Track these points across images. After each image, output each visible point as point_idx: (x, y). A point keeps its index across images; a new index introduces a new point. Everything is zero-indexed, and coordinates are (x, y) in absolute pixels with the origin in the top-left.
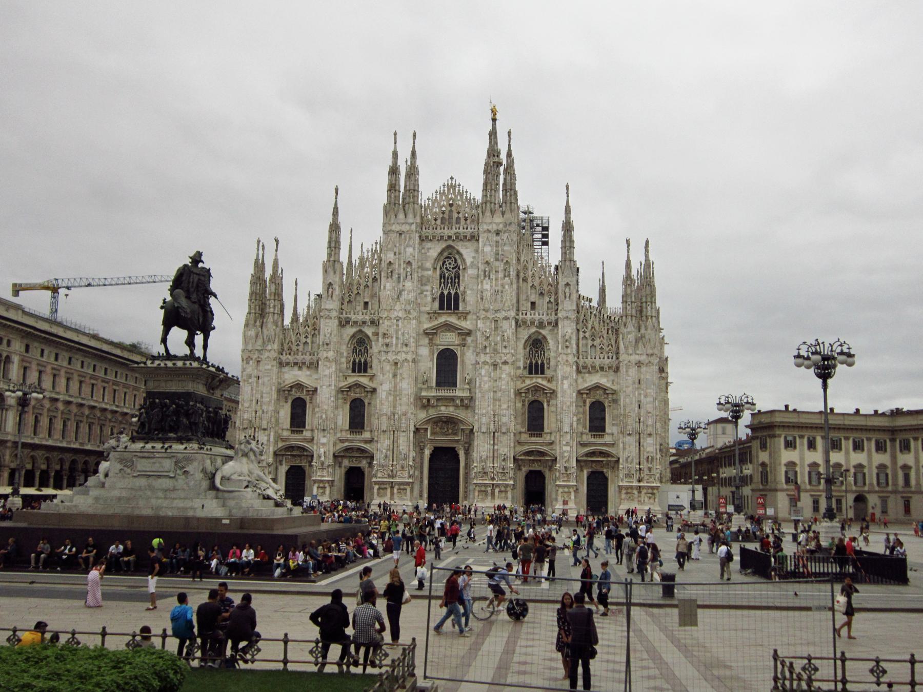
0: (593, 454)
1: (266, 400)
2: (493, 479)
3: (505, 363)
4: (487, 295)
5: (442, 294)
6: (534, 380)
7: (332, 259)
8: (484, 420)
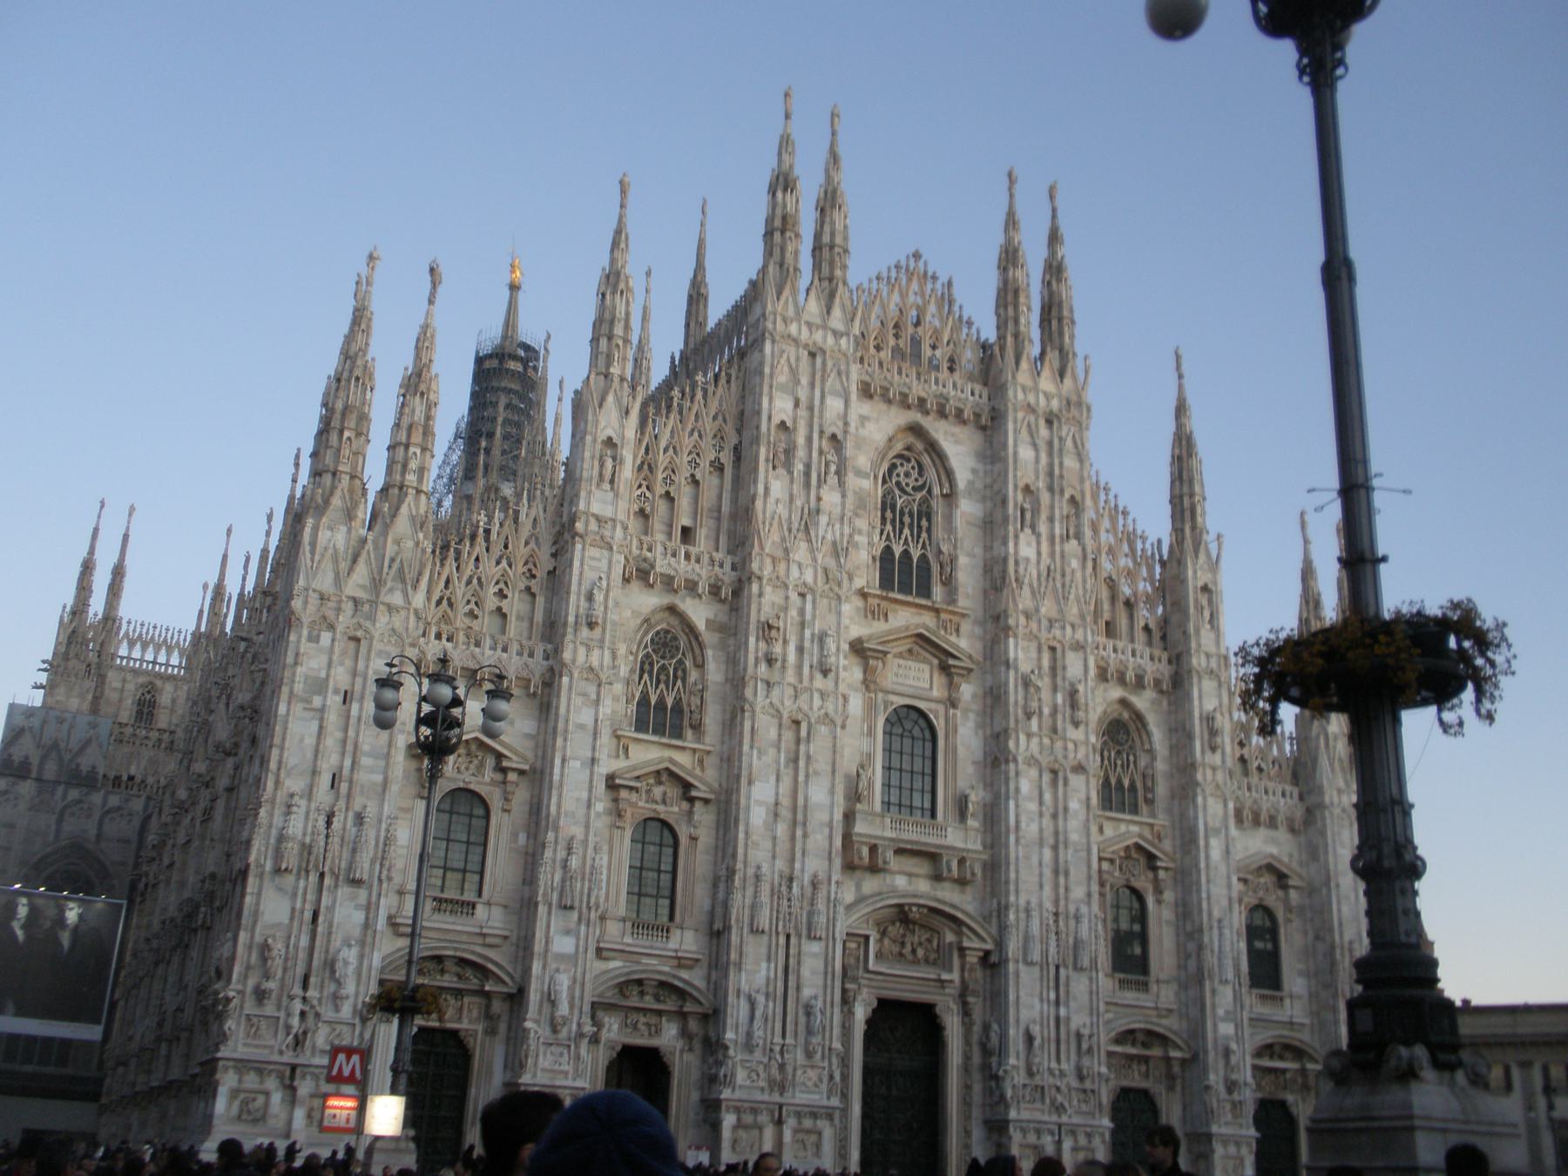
1: (368, 776)
2: (1059, 1109)
3: (1080, 768)
5: (888, 551)
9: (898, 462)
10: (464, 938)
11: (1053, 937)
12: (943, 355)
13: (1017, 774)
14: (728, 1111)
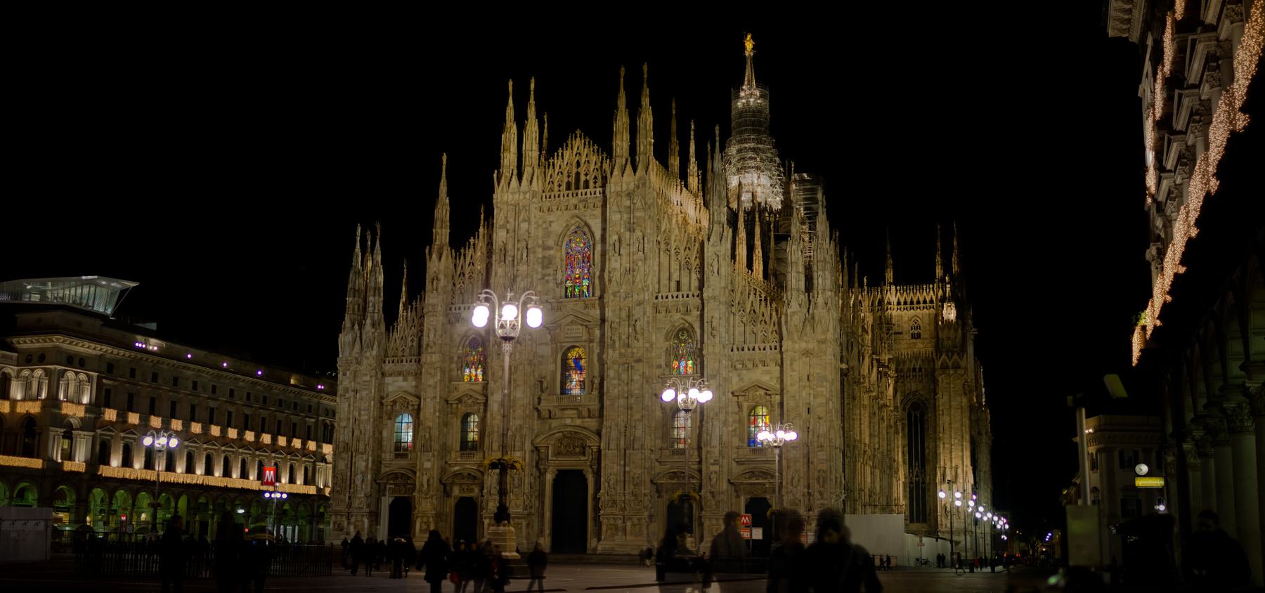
0: (752, 474)
1: (364, 418)
3: (639, 361)
4: (616, 276)
8: (614, 434)
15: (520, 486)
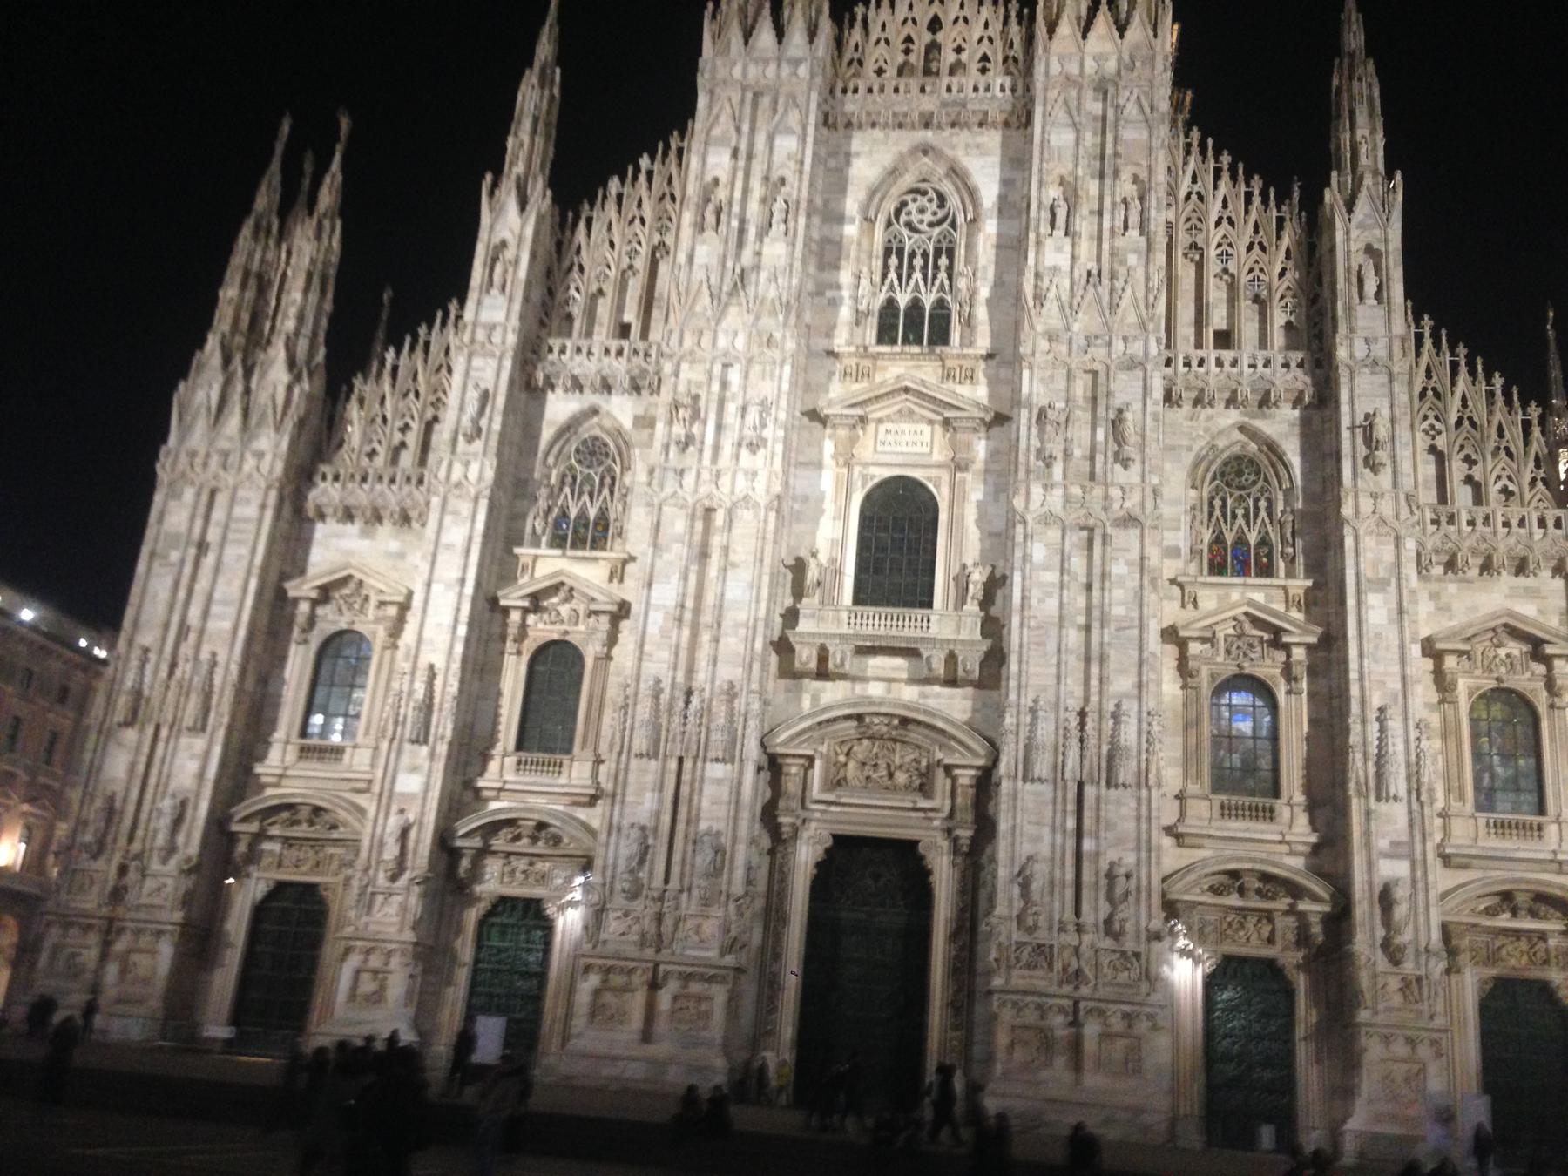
1: (221, 624)
3: (1129, 521)
6: (1235, 596)
7: (519, 169)
8: (1046, 731)
9: (909, 198)
10: (330, 785)
11: (1074, 743)
12: (971, 58)
13: (1025, 537)
14: (587, 969)
15: (716, 871)
